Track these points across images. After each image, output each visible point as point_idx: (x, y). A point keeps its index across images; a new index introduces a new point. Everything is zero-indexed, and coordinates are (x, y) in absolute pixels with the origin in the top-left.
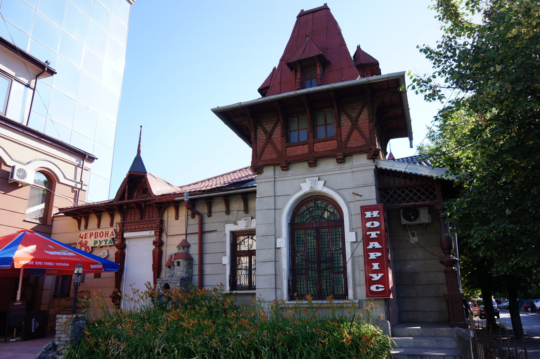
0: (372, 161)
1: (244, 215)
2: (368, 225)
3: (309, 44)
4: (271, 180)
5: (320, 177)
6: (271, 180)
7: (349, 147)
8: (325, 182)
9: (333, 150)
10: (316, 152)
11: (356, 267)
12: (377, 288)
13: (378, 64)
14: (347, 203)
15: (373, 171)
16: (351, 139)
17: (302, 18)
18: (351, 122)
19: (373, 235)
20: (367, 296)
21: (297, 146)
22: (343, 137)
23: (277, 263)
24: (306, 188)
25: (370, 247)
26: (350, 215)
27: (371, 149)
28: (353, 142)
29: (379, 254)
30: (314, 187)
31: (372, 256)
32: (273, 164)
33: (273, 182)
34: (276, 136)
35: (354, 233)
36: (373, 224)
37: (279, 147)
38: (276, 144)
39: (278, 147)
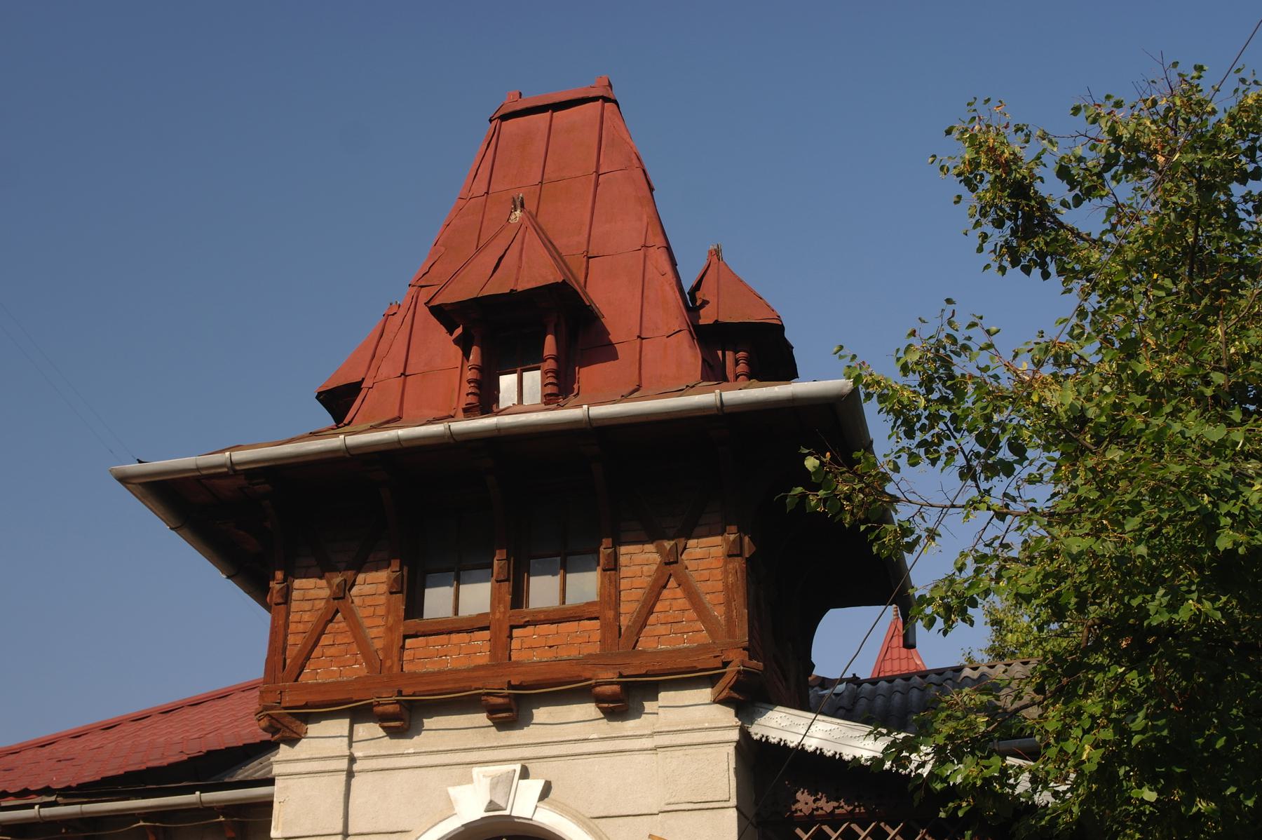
3: (519, 236)
5: (532, 767)
7: (643, 652)
10: (518, 663)
13: (781, 328)
15: (731, 749)
16: (652, 618)
21: (450, 633)
27: (726, 664)
28: (662, 629)
30: (503, 805)
33: (343, 777)
34: (367, 589)
37: (376, 633)
38: (367, 623)
39: (373, 633)
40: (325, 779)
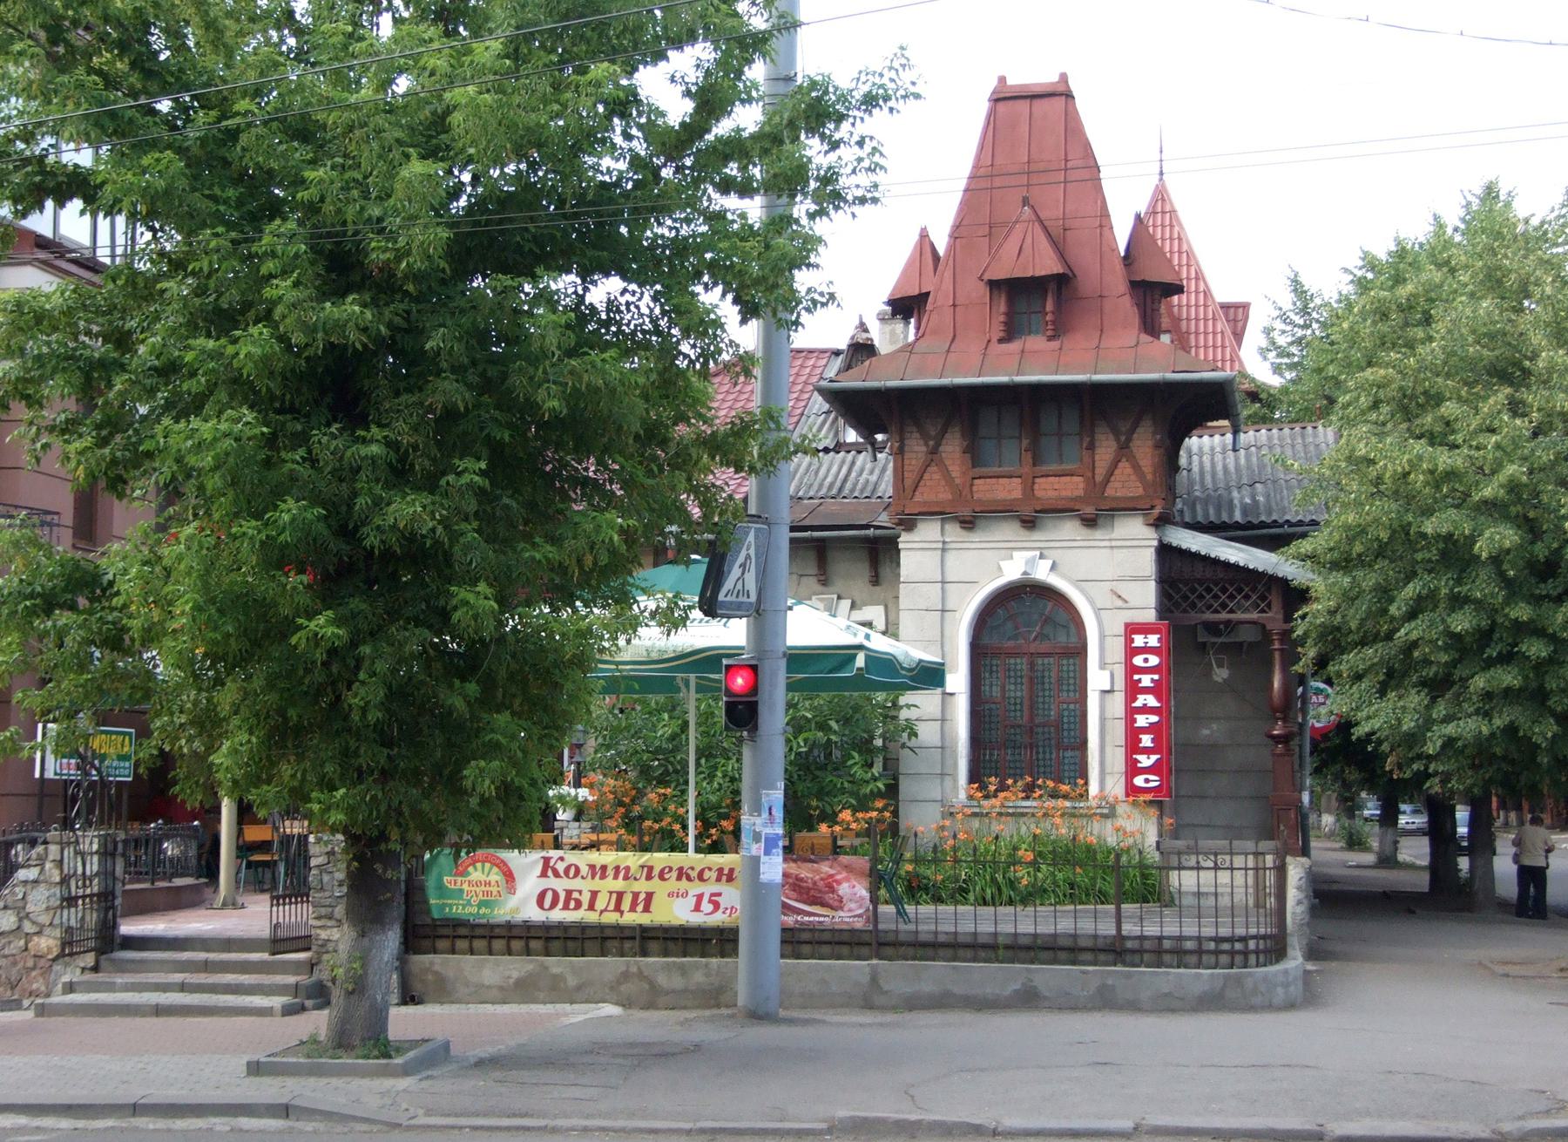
0: (1153, 529)
1: (820, 588)
2: (1138, 661)
4: (934, 545)
5: (1046, 552)
6: (934, 545)
8: (1054, 563)
9: (1075, 499)
10: (1038, 499)
11: (1108, 738)
12: (1147, 781)
14: (1098, 611)
15: (1153, 550)
16: (1113, 479)
17: (1001, 107)
18: (1117, 440)
19: (1146, 680)
20: (1127, 795)
22: (1097, 471)
23: (948, 724)
24: (1013, 569)
25: (1138, 704)
26: (1102, 637)
27: (1152, 507)
29: (1154, 719)
31: (1142, 721)
32: (939, 513)
35: (1107, 674)
36: (1146, 660)
40: (929, 553)
